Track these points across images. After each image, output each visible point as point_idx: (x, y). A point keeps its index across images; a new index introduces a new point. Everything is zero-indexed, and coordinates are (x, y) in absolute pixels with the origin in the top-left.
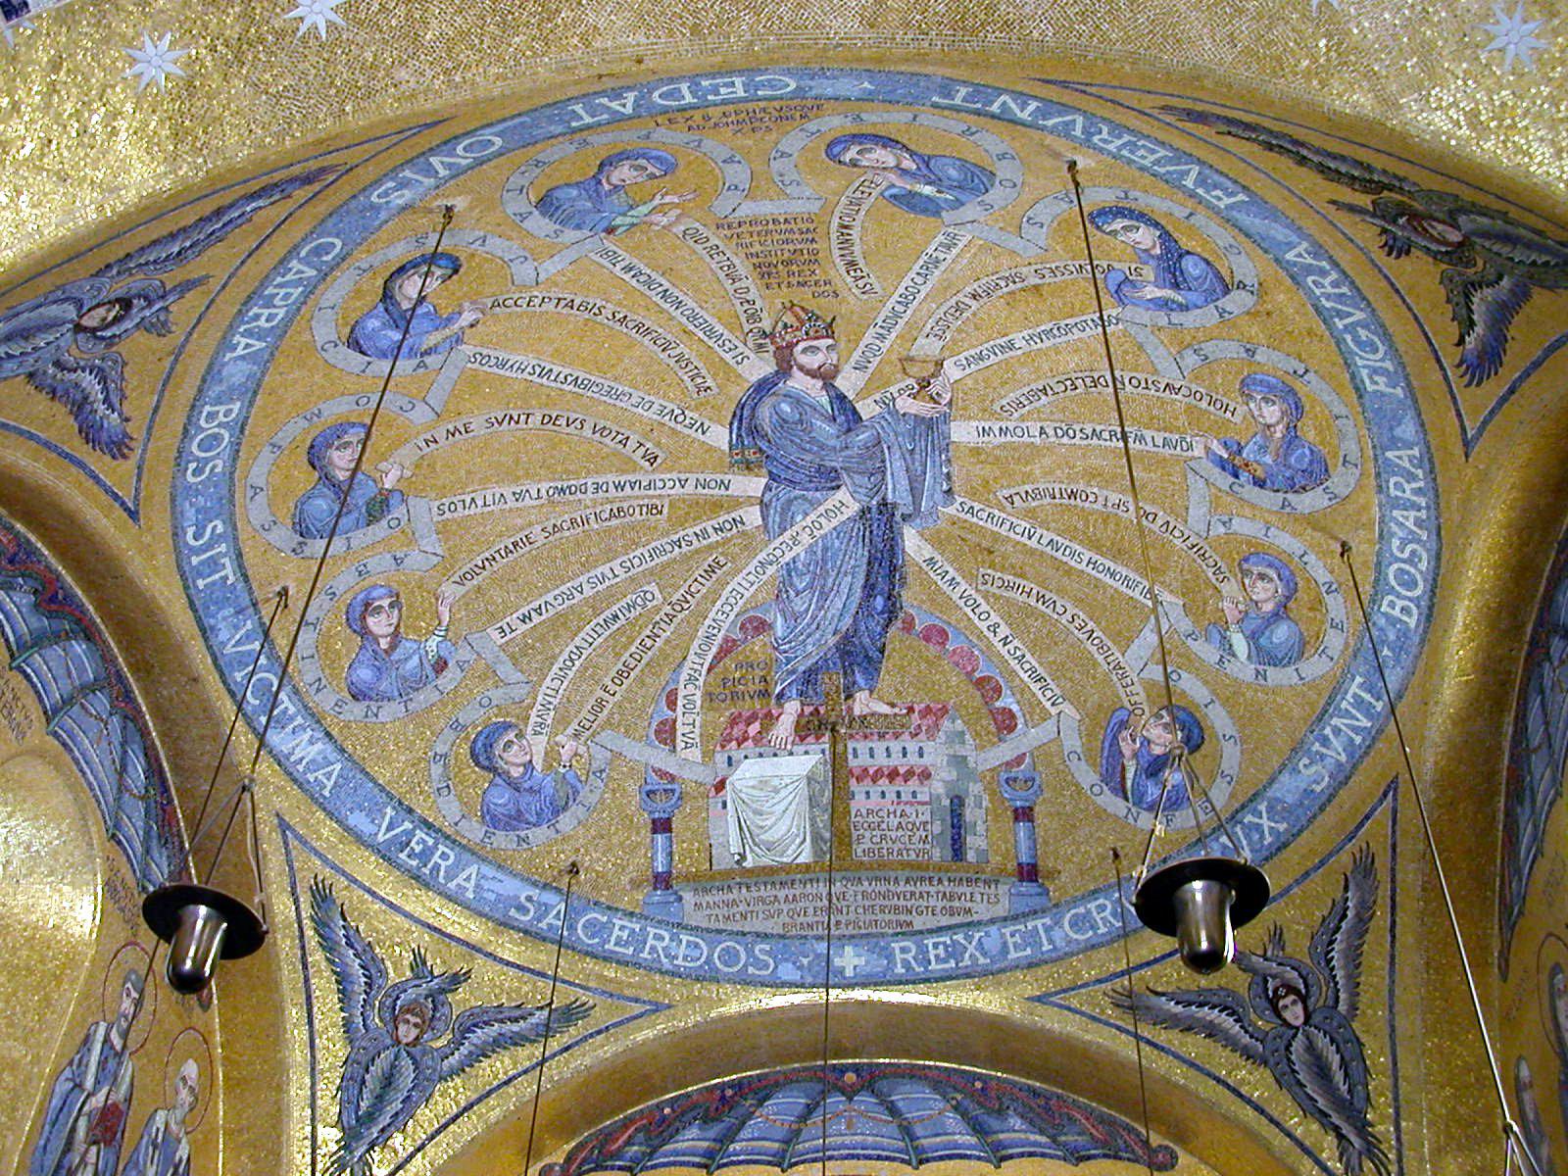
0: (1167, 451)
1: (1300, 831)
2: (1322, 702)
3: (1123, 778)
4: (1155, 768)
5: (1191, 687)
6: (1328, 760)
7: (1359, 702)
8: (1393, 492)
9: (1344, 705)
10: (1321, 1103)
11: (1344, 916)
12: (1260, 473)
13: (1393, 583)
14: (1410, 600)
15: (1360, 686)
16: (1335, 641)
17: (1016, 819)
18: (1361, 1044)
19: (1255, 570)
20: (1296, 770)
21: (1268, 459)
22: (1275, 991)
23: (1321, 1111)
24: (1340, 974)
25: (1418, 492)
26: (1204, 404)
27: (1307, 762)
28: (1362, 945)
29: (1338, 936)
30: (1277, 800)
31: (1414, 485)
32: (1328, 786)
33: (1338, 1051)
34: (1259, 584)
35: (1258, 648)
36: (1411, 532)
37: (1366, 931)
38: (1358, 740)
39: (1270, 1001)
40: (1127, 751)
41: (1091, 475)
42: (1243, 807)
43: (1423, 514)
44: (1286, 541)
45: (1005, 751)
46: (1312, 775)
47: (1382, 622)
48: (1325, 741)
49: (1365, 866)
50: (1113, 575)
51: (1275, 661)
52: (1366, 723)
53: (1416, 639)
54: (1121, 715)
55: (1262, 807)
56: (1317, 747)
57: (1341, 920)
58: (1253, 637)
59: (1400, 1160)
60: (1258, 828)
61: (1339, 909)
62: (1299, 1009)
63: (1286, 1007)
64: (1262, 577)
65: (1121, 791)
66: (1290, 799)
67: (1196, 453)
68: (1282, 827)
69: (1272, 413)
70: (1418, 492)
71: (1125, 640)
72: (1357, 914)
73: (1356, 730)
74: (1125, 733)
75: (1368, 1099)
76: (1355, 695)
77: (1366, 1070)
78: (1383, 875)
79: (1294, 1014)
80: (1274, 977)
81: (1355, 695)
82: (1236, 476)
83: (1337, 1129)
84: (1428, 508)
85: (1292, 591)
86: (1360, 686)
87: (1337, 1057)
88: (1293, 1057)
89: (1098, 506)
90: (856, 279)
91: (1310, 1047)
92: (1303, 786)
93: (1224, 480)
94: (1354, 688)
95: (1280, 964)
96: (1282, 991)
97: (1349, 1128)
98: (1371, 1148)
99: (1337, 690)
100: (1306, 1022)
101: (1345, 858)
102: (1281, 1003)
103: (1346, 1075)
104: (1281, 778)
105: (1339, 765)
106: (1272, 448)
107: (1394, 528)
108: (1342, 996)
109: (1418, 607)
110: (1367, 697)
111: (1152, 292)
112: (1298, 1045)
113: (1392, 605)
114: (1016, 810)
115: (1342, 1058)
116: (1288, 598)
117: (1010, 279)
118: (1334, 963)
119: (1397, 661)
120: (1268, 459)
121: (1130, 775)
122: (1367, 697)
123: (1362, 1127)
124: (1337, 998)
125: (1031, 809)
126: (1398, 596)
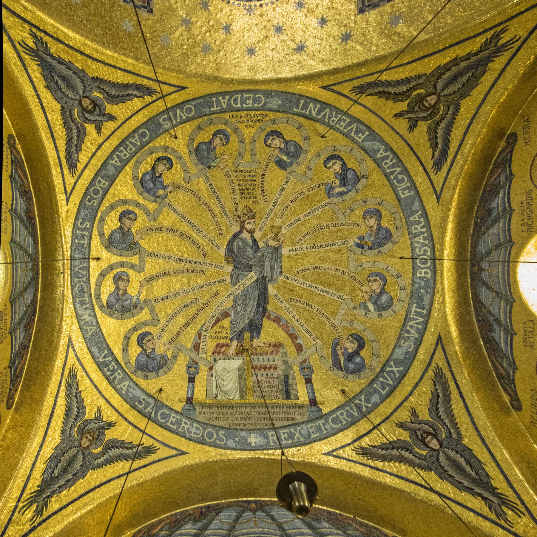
0: (342, 246)
1: (409, 368)
2: (403, 317)
3: (340, 363)
4: (350, 357)
5: (358, 327)
6: (411, 338)
7: (417, 313)
8: (414, 232)
9: (412, 316)
11: (438, 397)
12: (370, 244)
13: (419, 265)
14: (427, 268)
15: (416, 307)
16: (403, 295)
17: (306, 383)
19: (372, 279)
20: (400, 346)
21: (372, 239)
22: (422, 436)
25: (423, 227)
26: (352, 227)
27: (403, 341)
30: (396, 359)
31: (421, 225)
32: (414, 348)
34: (374, 283)
35: (377, 306)
36: (422, 243)
37: (450, 400)
38: (420, 327)
39: (421, 441)
40: (340, 353)
41: (321, 260)
42: (384, 365)
43: (425, 235)
44: (381, 265)
45: (301, 359)
46: (407, 345)
47: (418, 281)
48: (408, 332)
49: (439, 375)
50: (328, 293)
51: (384, 309)
52: (421, 320)
53: (432, 281)
54: (336, 341)
55: (392, 363)
56: (406, 335)
58: (375, 303)
60: (392, 371)
61: (435, 395)
64: (375, 281)
65: (340, 368)
66: (401, 357)
67: (351, 244)
68: (401, 369)
69: (372, 221)
70: (423, 227)
71: (334, 314)
72: (443, 394)
73: (418, 324)
74: (338, 347)
76: (415, 311)
78: (448, 375)
81: (415, 311)
82: (363, 248)
84: (427, 231)
85: (385, 281)
86: (416, 307)
89: (323, 270)
90: (264, 196)
92: (405, 351)
93: (359, 250)
94: (414, 309)
99: (408, 312)
101: (431, 373)
104: (396, 351)
105: (416, 338)
106: (373, 233)
107: (416, 245)
109: (430, 269)
110: (419, 310)
111: (338, 190)
113: (421, 273)
114: (306, 379)
116: (384, 285)
117: (301, 194)
119: (427, 292)
120: (372, 239)
121: (342, 362)
122: (419, 310)
125: (311, 378)
126: (422, 269)
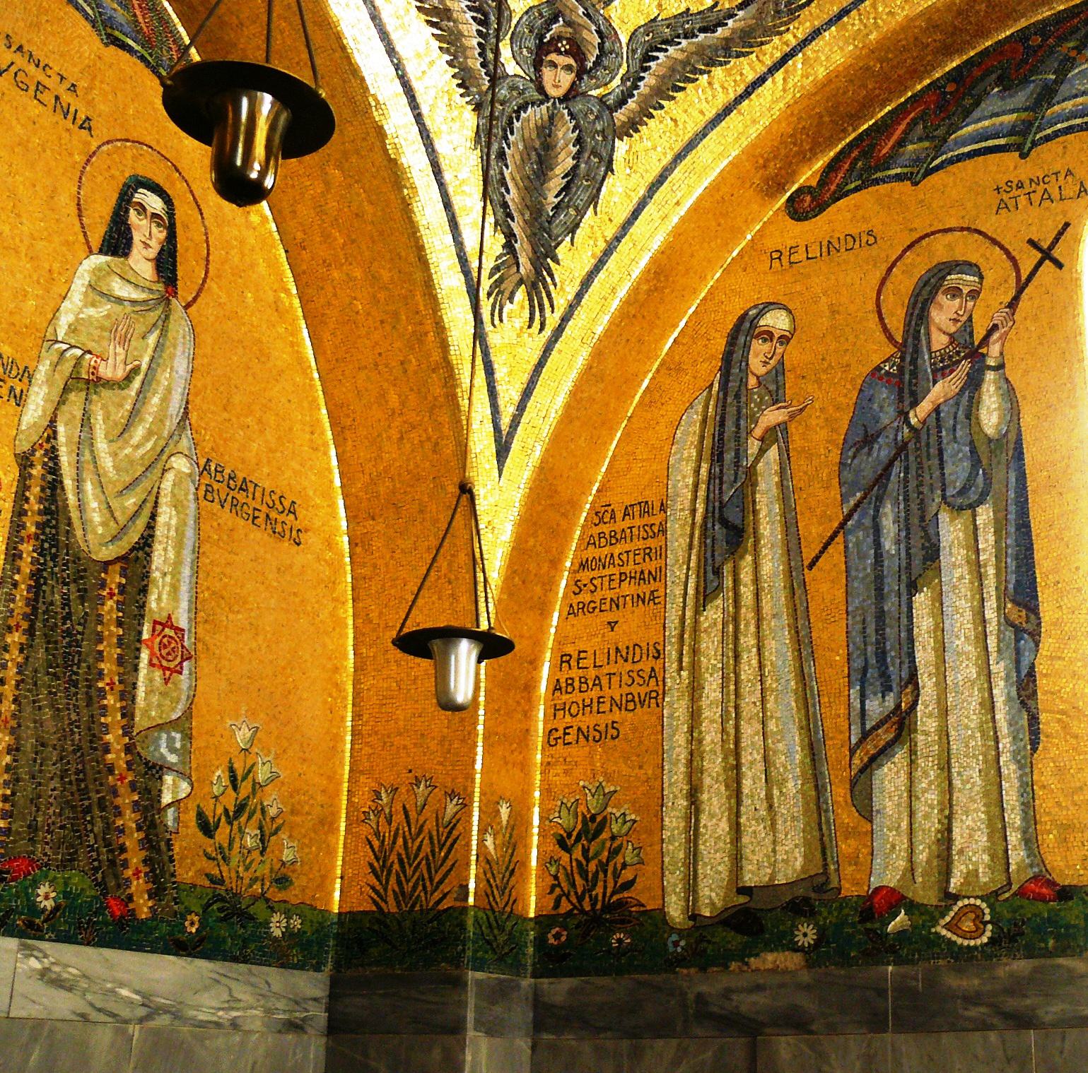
10: (513, 197)
18: (610, 168)
23: (505, 205)
24: (649, 80)
28: (702, 72)
29: (684, 42)
33: (577, 157)
57: (704, 30)
59: (565, 319)
61: (713, 17)
62: (566, 79)
63: (554, 65)
75: (573, 229)
77: (594, 199)
79: (558, 80)
80: (568, 24)
83: (510, 236)
87: (570, 162)
88: (517, 125)
91: (546, 131)
95: (588, 15)
96: (564, 45)
97: (527, 246)
98: (538, 285)
100: (565, 99)
102: (553, 57)
103: (566, 188)
108: (632, 104)
112: (534, 114)
115: (575, 167)
118: (653, 64)
123: (544, 255)
124: (622, 102)
